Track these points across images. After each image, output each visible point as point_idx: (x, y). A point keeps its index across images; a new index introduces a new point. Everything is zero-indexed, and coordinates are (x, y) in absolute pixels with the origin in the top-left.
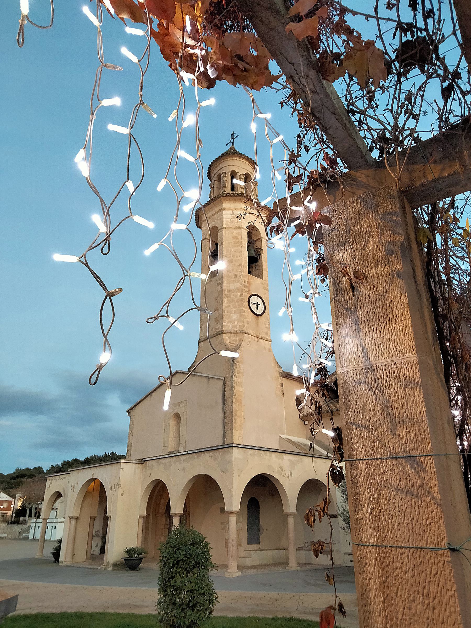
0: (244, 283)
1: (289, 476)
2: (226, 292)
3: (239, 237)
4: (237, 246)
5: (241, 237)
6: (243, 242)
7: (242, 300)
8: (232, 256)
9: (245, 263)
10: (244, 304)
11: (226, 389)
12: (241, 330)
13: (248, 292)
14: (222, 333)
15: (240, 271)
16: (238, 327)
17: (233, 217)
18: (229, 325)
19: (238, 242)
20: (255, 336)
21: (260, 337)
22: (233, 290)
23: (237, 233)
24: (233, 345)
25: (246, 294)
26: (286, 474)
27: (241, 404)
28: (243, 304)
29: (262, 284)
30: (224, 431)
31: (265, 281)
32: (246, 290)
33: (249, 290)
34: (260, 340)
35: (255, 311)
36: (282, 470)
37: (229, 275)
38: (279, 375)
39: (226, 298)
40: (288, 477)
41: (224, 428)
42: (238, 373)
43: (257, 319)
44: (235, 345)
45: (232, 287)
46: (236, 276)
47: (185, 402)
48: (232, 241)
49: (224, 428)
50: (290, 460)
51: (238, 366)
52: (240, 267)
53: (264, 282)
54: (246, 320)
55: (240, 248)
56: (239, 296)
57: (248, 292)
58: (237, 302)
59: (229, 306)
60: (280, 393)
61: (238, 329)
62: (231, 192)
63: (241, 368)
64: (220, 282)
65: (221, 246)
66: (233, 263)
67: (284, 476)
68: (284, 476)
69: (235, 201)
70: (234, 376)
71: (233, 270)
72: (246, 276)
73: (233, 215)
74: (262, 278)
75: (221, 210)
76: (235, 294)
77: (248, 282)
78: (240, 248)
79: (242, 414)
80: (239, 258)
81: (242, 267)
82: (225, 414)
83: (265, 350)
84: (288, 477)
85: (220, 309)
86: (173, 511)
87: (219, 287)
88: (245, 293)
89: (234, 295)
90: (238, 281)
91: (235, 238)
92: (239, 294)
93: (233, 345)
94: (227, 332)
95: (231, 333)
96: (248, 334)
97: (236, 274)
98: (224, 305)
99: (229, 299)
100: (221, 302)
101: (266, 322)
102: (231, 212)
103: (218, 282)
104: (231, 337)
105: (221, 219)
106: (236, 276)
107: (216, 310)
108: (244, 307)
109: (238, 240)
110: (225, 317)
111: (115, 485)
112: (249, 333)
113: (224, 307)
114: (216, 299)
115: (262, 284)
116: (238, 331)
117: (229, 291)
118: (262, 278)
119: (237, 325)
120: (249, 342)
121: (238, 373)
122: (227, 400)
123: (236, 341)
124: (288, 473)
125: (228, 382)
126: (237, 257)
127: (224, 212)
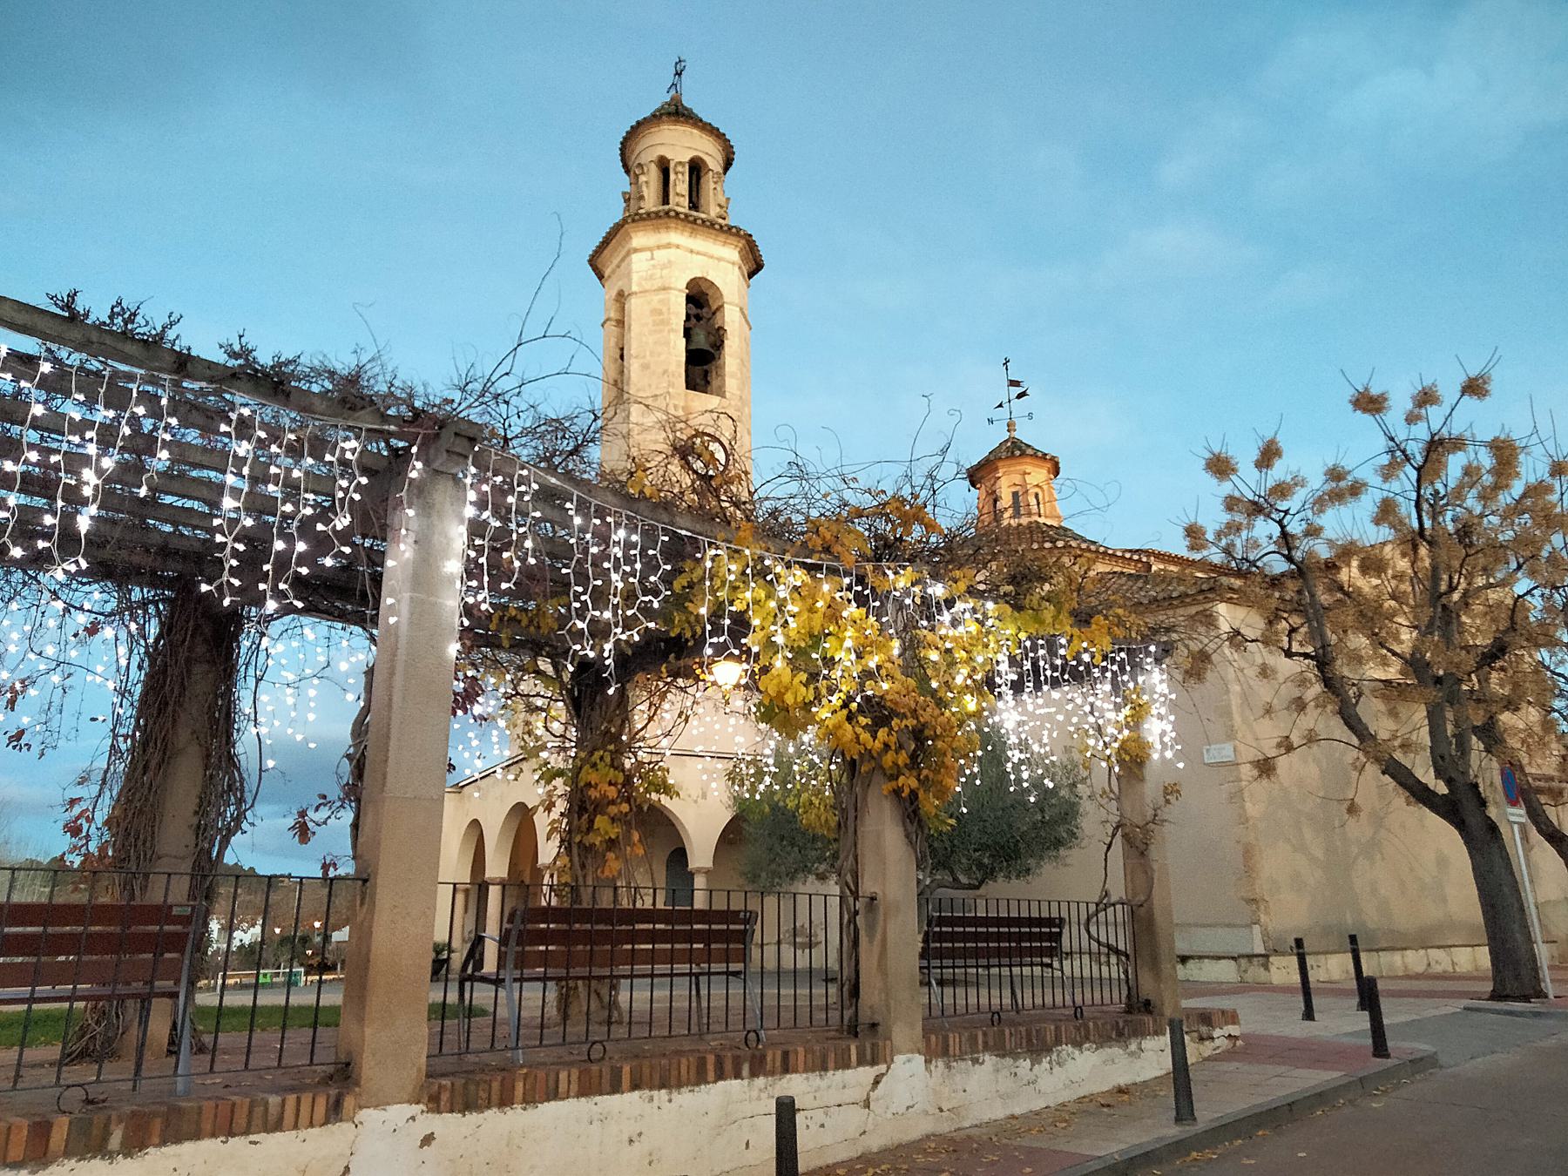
4: (661, 331)
9: (679, 365)
19: (663, 322)
23: (660, 301)
55: (665, 333)
62: (661, 208)
69: (657, 229)
74: (724, 396)
75: (628, 254)
80: (663, 357)
102: (648, 254)
118: (724, 396)
126: (659, 355)
127: (635, 257)
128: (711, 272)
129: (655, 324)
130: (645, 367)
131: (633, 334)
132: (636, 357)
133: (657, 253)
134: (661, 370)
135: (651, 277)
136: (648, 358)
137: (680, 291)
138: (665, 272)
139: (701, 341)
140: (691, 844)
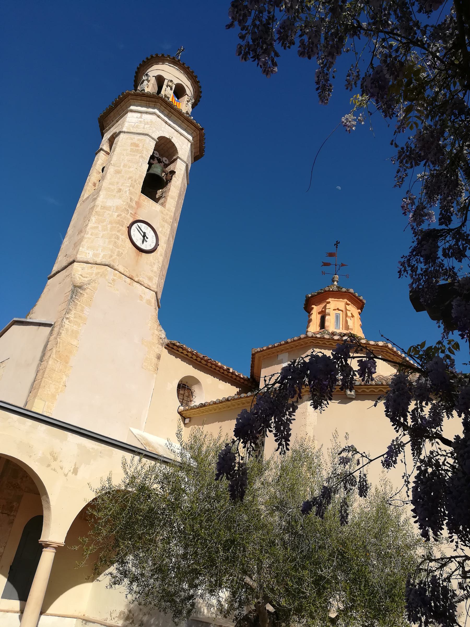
0: (129, 200)
1: (70, 474)
2: (98, 209)
3: (140, 145)
5: (143, 145)
6: (145, 152)
7: (118, 223)
8: (122, 166)
10: (121, 228)
14: (74, 261)
15: (128, 185)
16: (101, 256)
18: (88, 252)
20: (128, 275)
21: (136, 280)
22: (110, 207)
25: (128, 216)
26: (62, 468)
27: (67, 363)
28: (118, 227)
29: (163, 213)
30: (27, 400)
31: (168, 210)
32: (130, 211)
33: (135, 213)
35: (139, 243)
37: (109, 188)
38: (157, 342)
41: (29, 396)
42: (75, 317)
45: (110, 203)
48: (129, 148)
52: (130, 181)
53: (166, 211)
54: (117, 250)
55: (137, 157)
56: (115, 216)
58: (111, 223)
59: (97, 227)
61: (99, 259)
63: (85, 312)
66: (121, 175)
68: (54, 470)
70: (67, 318)
71: (118, 183)
72: (136, 193)
73: (140, 119)
76: (110, 213)
78: (137, 157)
80: (131, 169)
81: (132, 181)
82: (37, 374)
84: (66, 475)
88: (127, 214)
89: (109, 214)
90: (120, 197)
92: (116, 214)
93: (85, 279)
94: (81, 260)
95: (87, 263)
96: (115, 270)
98: (90, 225)
99: (101, 217)
101: (154, 264)
104: (86, 269)
106: (120, 190)
107: (80, 232)
108: (118, 231)
109: (137, 148)
110: (85, 240)
112: (116, 267)
113: (88, 227)
115: (163, 213)
116: (99, 262)
117: (104, 208)
119: (100, 254)
120: (113, 280)
121: (75, 317)
123: (92, 274)
124: (68, 467)
126: (129, 167)
128: (174, 138)
129: (132, 150)
130: (118, 172)
131: (115, 153)
132: (114, 165)
133: (144, 116)
134: (128, 176)
135: (137, 127)
136: (122, 167)
137: (153, 139)
138: (147, 126)
139: (157, 170)
140: (49, 508)
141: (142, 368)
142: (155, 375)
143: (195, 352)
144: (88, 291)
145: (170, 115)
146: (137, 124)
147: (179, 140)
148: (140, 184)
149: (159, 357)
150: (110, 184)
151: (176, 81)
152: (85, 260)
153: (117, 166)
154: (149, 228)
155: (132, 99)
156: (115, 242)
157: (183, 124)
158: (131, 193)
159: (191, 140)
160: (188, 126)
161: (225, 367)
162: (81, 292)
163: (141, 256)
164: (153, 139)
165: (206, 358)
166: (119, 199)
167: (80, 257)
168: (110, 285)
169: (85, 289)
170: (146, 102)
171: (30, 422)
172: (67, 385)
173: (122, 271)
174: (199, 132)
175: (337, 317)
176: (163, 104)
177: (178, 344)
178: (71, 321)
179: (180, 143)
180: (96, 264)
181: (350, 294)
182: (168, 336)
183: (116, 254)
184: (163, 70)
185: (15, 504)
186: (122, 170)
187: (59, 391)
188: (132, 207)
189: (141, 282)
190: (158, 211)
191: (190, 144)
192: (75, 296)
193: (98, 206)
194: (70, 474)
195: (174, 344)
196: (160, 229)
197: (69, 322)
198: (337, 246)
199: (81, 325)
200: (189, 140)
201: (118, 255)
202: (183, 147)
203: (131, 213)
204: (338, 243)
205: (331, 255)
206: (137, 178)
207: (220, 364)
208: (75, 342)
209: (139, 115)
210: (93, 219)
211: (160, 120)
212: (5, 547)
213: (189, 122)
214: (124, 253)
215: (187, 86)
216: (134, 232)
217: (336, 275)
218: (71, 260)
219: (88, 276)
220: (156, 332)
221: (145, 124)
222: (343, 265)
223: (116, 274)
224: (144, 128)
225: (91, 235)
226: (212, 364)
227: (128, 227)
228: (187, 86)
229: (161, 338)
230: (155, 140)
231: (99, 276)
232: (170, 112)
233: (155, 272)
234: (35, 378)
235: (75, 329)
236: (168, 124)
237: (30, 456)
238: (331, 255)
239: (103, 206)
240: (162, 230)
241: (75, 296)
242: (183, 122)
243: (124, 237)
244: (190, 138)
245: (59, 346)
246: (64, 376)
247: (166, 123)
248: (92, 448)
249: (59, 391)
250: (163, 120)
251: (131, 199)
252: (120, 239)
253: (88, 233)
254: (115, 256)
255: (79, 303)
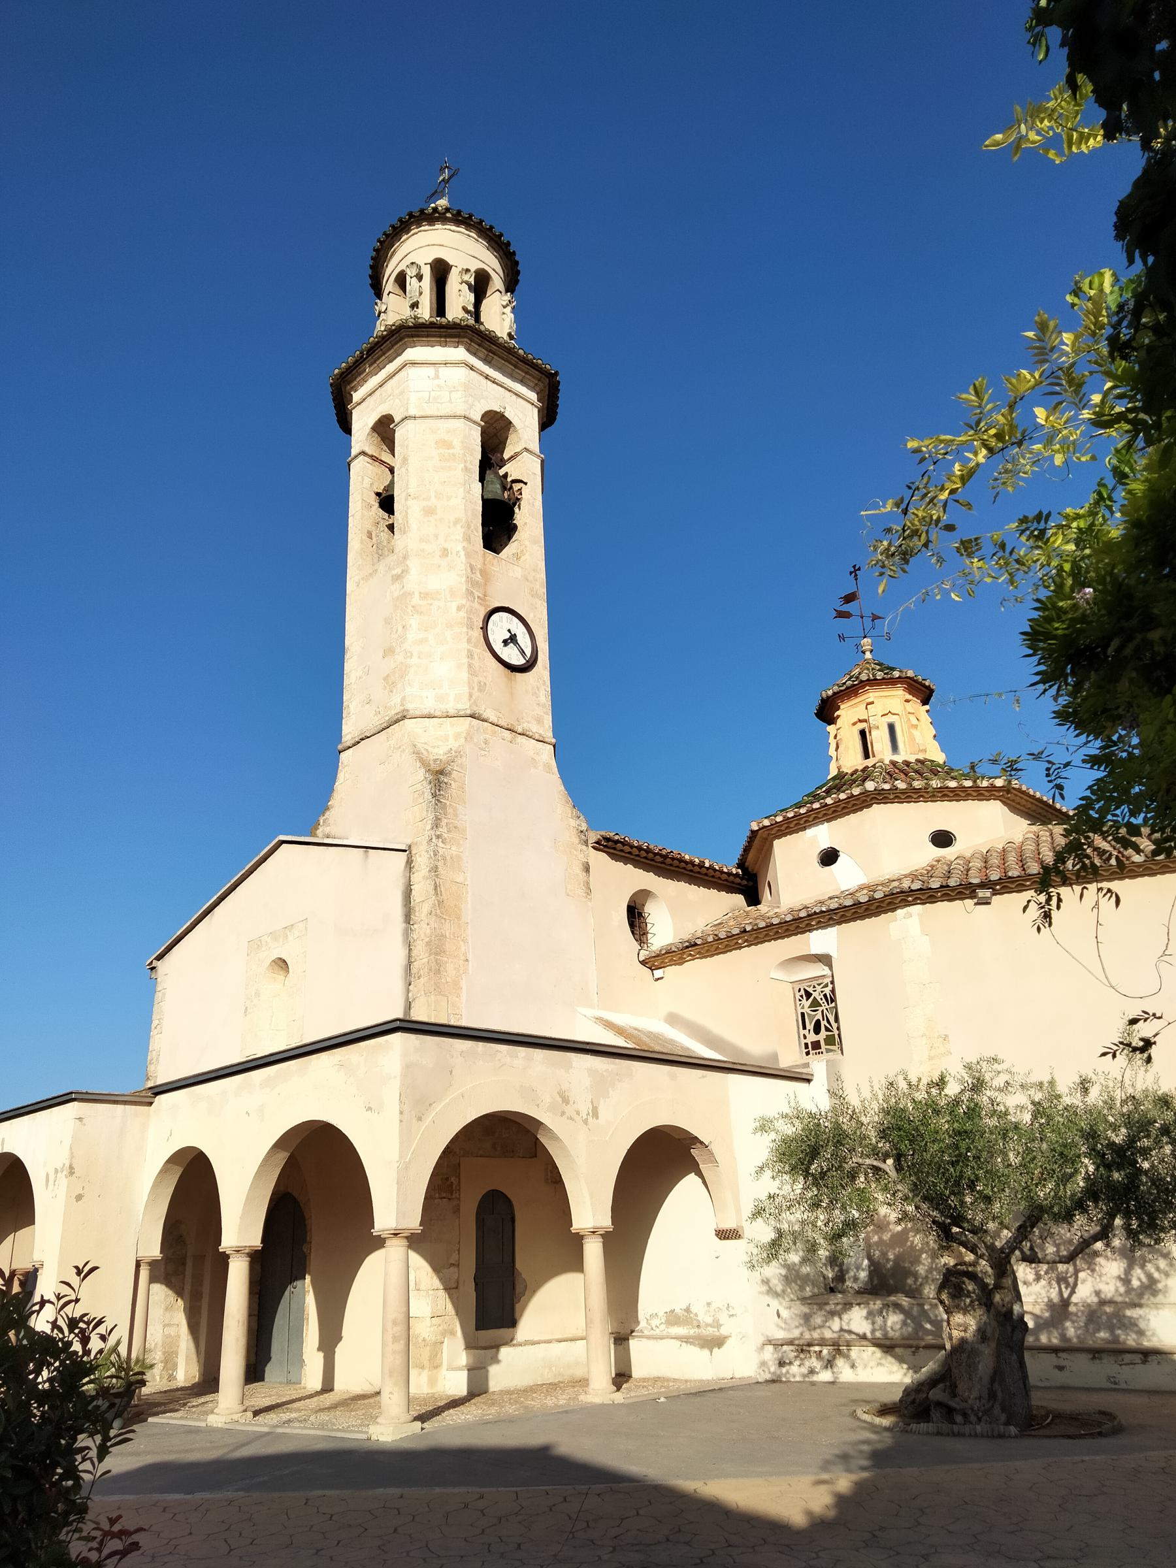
1: (590, 1119)
11: (414, 878)
12: (460, 706)
13: (483, 599)
15: (458, 537)
17: (439, 386)
20: (506, 726)
21: (520, 730)
24: (436, 751)
25: (476, 605)
26: (578, 1113)
27: (459, 918)
32: (477, 594)
34: (521, 739)
36: (566, 1101)
37: (423, 550)
38: (577, 841)
39: (416, 616)
40: (586, 1122)
41: (408, 991)
43: (510, 680)
44: (441, 752)
46: (445, 553)
47: (301, 925)
49: (408, 991)
50: (592, 1072)
51: (450, 810)
57: (483, 599)
60: (581, 892)
64: (398, 571)
65: (403, 469)
67: (571, 1118)
68: (571, 1118)
71: (436, 536)
73: (436, 382)
77: (484, 573)
79: (463, 949)
82: (410, 950)
83: (535, 767)
84: (586, 1122)
85: (398, 650)
86: (229, 1240)
87: (397, 586)
91: (445, 444)
92: (454, 605)
94: (418, 713)
96: (483, 720)
97: (447, 546)
98: (412, 635)
100: (400, 629)
103: (394, 572)
105: (402, 393)
109: (451, 451)
111: (56, 1171)
112: (485, 715)
114: (388, 621)
115: (527, 580)
116: (452, 712)
117: (425, 596)
122: (417, 909)
124: (585, 1108)
125: (420, 856)
126: (449, 498)
130: (429, 511)
133: (443, 370)
137: (475, 422)
138: (454, 395)
139: (495, 490)
141: (568, 895)
142: (589, 903)
143: (646, 844)
144: (454, 774)
145: (489, 359)
146: (433, 394)
147: (516, 408)
148: (477, 531)
149: (587, 869)
150: (421, 540)
151: (474, 266)
152: (425, 712)
153: (424, 499)
154: (514, 618)
155: (408, 336)
156: (470, 666)
157: (517, 370)
158: (468, 555)
159: (536, 401)
160: (526, 373)
161: (697, 861)
162: (446, 780)
163: (515, 680)
164: (475, 422)
165: (664, 852)
166: (449, 571)
167: (412, 707)
168: (482, 752)
169: (450, 773)
170: (438, 339)
171: (522, 1051)
172: (470, 957)
173: (495, 721)
174: (547, 380)
175: (891, 728)
176: (476, 338)
177: (617, 838)
178: (445, 839)
179: (521, 416)
180: (447, 717)
181: (909, 680)
182: (591, 827)
183: (476, 689)
184: (443, 246)
185: (453, 1179)
186: (435, 506)
187: (461, 972)
188: (477, 583)
189: (528, 733)
190: (520, 577)
191: (536, 411)
192: (439, 790)
193: (413, 593)
194: (590, 1119)
195: (608, 839)
196: (532, 615)
197: (442, 842)
198: (856, 575)
199: (461, 842)
200: (533, 404)
201: (480, 690)
202: (527, 423)
203: (478, 597)
204: (855, 571)
205: (849, 598)
206: (469, 520)
207: (687, 857)
208: (460, 879)
209: (430, 371)
210: (414, 622)
211: (475, 373)
212: (459, 1251)
213: (528, 365)
214: (487, 683)
215: (494, 270)
216: (497, 633)
217: (865, 637)
218: (392, 713)
219: (441, 743)
220: (573, 823)
221: (450, 392)
222: (875, 618)
223: (487, 728)
224: (450, 401)
225: (419, 657)
226: (673, 859)
227: (482, 628)
228: (494, 270)
229: (582, 832)
230: (479, 425)
231: (463, 740)
232: (490, 351)
233: (544, 706)
234: (410, 956)
235: (455, 853)
236: (491, 381)
237: (538, 1105)
238: (849, 598)
239: (422, 591)
240: (535, 616)
241: (439, 790)
242: (515, 366)
243: (479, 651)
244: (533, 396)
245: (441, 891)
246: (462, 943)
247: (487, 377)
248: (607, 1071)
249: (461, 972)
250: (481, 373)
251: (472, 567)
252: (475, 656)
253: (412, 655)
254: (476, 694)
255: (448, 803)
